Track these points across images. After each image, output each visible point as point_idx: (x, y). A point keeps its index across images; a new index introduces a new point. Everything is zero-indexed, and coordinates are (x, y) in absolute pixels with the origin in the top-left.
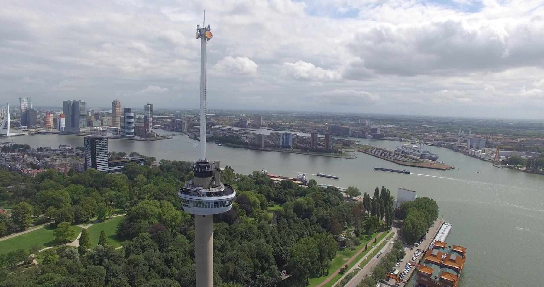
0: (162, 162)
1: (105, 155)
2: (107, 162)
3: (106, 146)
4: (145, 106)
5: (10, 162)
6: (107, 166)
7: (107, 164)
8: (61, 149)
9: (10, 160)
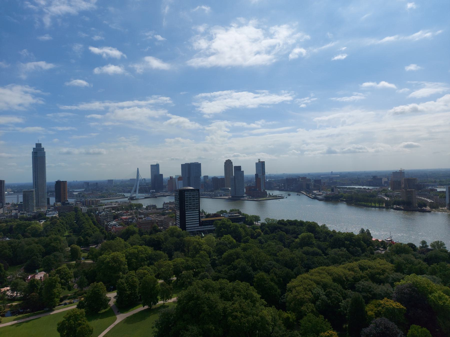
0: (267, 222)
1: (195, 211)
2: (198, 220)
3: (198, 199)
4: (256, 163)
5: (111, 219)
6: (198, 225)
7: (198, 223)
8: (165, 208)
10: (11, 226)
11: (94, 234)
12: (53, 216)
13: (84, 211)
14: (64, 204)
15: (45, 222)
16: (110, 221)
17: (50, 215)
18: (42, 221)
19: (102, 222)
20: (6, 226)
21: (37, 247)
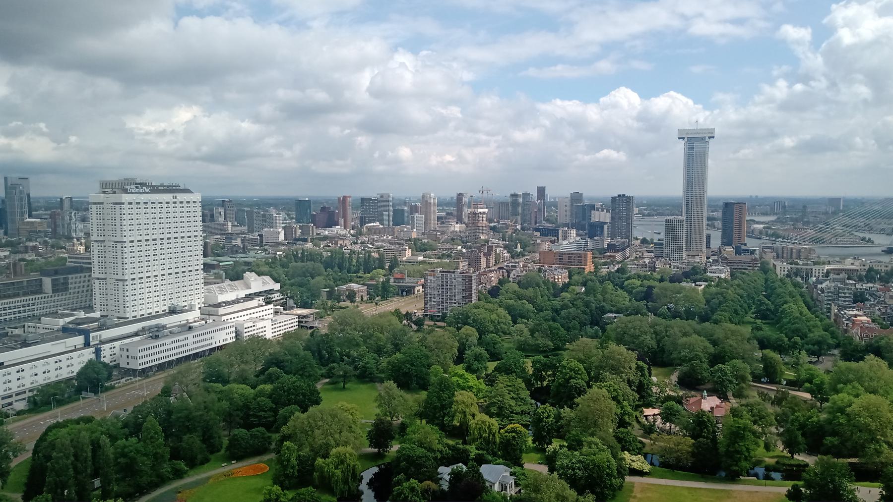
5: (847, 301)
9: (847, 297)
10: (650, 288)
11: (811, 335)
12: (719, 275)
13: (781, 271)
14: (738, 251)
15: (707, 287)
16: (846, 308)
17: (714, 273)
18: (701, 283)
19: (825, 306)
20: (641, 286)
21: (699, 342)
